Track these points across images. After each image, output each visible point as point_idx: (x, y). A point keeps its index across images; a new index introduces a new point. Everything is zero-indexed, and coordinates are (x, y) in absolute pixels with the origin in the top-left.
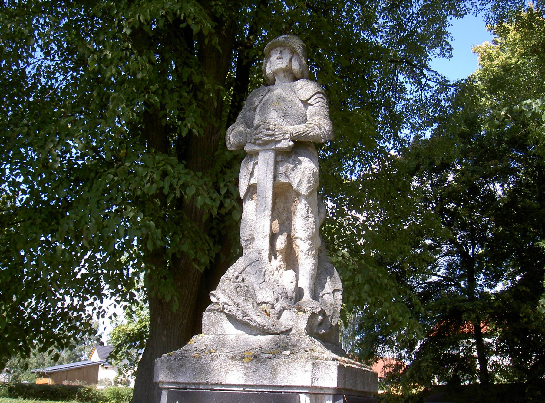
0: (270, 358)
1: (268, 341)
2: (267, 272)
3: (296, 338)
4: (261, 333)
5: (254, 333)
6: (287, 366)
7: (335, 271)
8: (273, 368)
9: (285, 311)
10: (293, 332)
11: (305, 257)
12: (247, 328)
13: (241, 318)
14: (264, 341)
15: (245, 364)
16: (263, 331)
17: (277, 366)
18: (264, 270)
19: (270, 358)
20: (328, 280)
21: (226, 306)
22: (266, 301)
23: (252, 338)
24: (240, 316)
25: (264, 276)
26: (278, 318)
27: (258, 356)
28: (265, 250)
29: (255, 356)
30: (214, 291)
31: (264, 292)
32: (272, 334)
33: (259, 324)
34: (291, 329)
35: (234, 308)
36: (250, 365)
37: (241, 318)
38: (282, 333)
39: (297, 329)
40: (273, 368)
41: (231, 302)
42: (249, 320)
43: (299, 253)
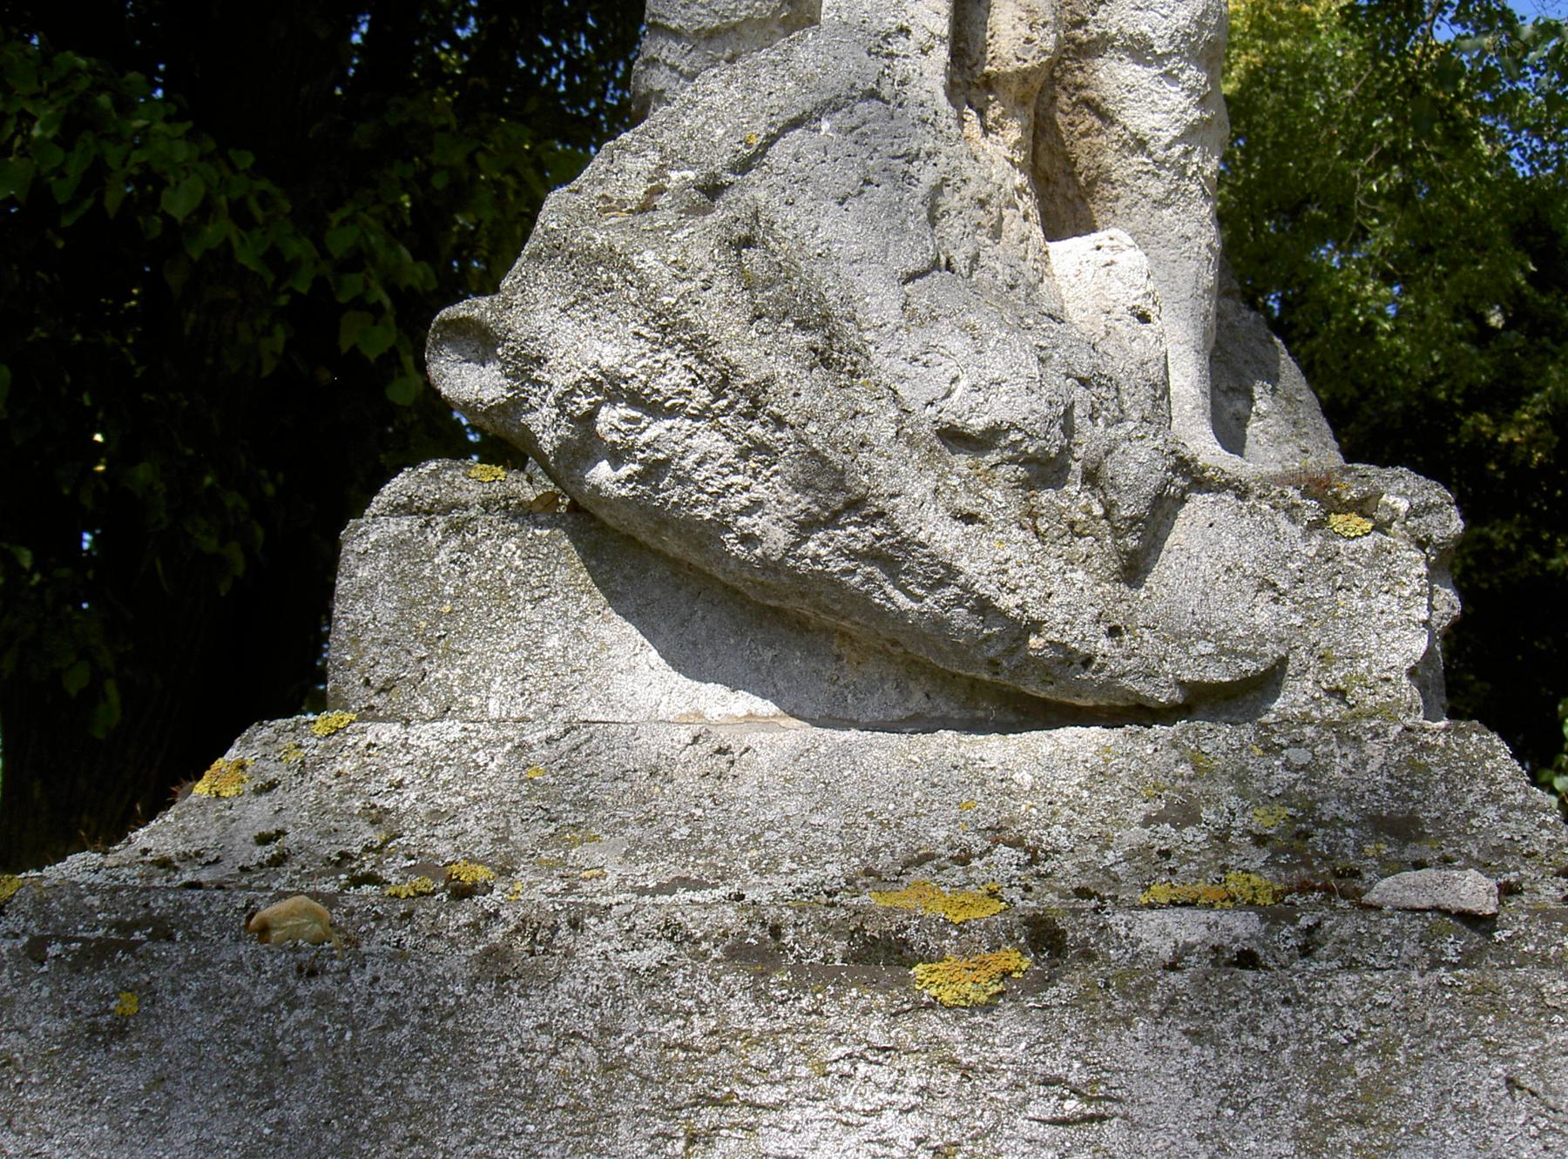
0: (1247, 960)
1: (1070, 783)
2: (950, 201)
3: (1374, 748)
4: (943, 707)
5: (864, 719)
6: (1525, 1052)
7: (1284, 356)
8: (1325, 1078)
9: (1199, 507)
10: (1293, 698)
11: (1156, 189)
12: (796, 662)
13: (778, 538)
14: (1025, 778)
15: (933, 1024)
16: (1007, 682)
17: (1383, 1050)
18: (928, 176)
19: (1247, 960)
20: (1261, 406)
21: (610, 418)
22: (978, 424)
23: (886, 756)
24: (765, 516)
25: (933, 220)
26: (1133, 570)
27: (1077, 932)
28: (918, 35)
29: (1044, 937)
30: (484, 302)
31: (957, 344)
32: (1111, 717)
33: (984, 607)
34: (1269, 681)
35: (707, 440)
36: (1009, 1038)
37: (778, 538)
38: (1201, 701)
39: (1337, 675)
40: (1325, 1078)
41: (674, 378)
42: (872, 556)
43: (1109, 159)
